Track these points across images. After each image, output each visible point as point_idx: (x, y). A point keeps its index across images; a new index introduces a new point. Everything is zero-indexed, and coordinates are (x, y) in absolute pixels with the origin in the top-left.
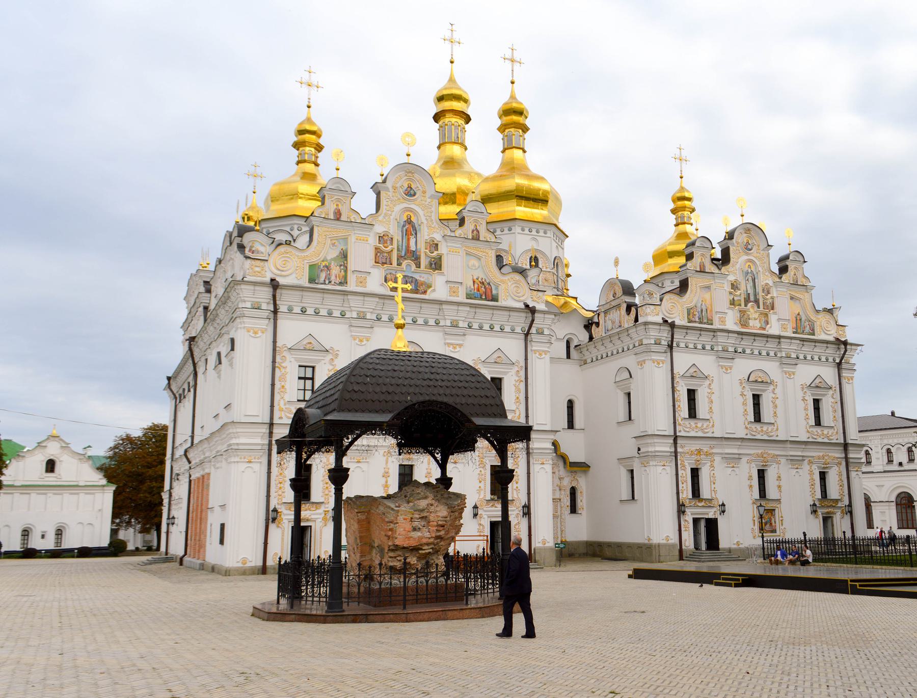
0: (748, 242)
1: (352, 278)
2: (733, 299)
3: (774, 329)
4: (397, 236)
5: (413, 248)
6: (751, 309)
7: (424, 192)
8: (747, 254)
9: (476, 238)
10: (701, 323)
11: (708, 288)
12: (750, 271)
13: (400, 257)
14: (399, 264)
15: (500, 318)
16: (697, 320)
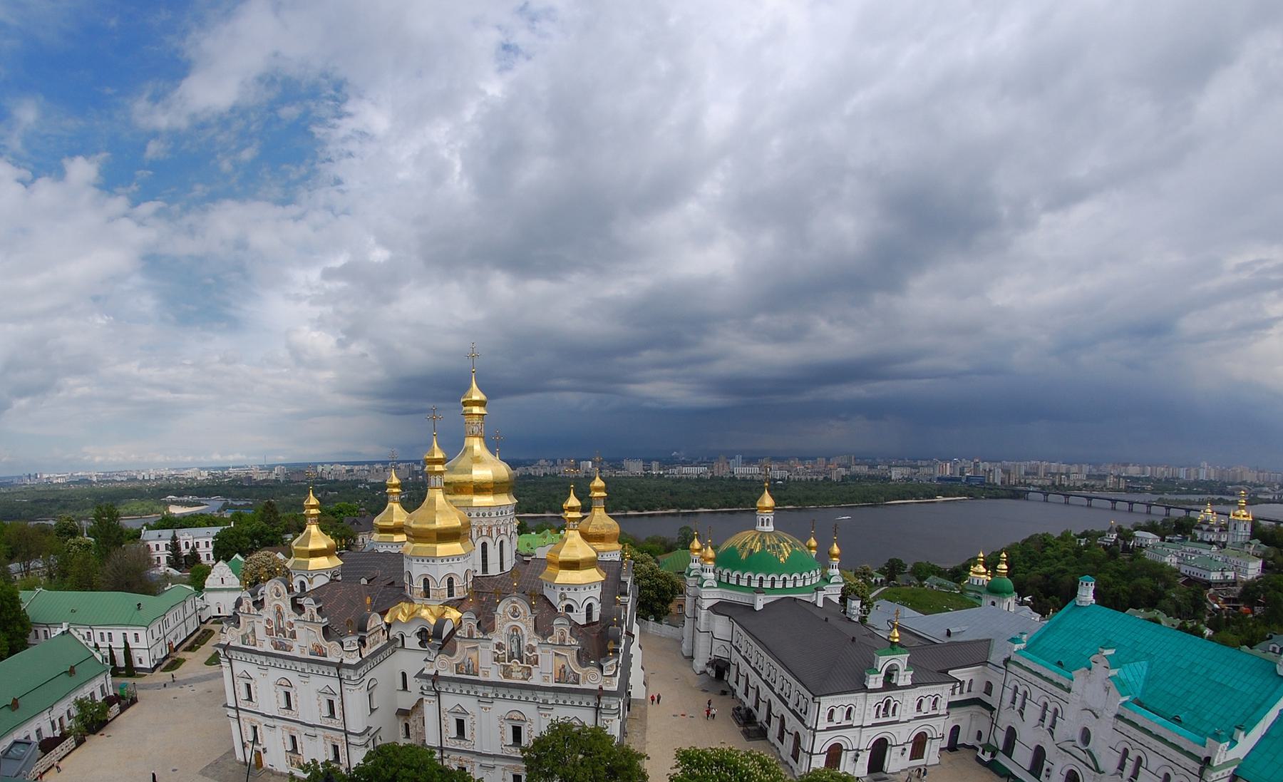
0: (515, 609)
1: (257, 642)
2: (498, 656)
3: (536, 680)
4: (274, 621)
5: (282, 627)
6: (515, 665)
7: (284, 593)
8: (513, 621)
9: (312, 620)
10: (467, 674)
11: (476, 648)
12: (515, 633)
13: (276, 631)
14: (277, 635)
15: (325, 668)
16: (464, 672)
